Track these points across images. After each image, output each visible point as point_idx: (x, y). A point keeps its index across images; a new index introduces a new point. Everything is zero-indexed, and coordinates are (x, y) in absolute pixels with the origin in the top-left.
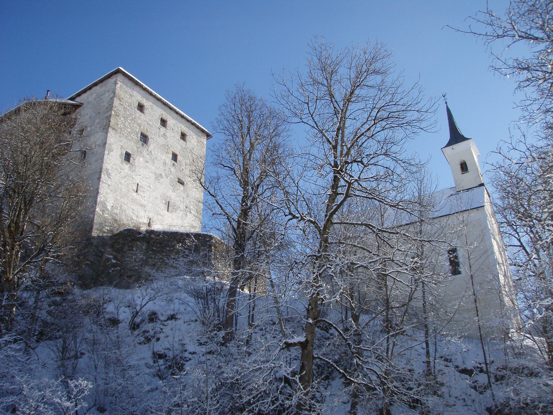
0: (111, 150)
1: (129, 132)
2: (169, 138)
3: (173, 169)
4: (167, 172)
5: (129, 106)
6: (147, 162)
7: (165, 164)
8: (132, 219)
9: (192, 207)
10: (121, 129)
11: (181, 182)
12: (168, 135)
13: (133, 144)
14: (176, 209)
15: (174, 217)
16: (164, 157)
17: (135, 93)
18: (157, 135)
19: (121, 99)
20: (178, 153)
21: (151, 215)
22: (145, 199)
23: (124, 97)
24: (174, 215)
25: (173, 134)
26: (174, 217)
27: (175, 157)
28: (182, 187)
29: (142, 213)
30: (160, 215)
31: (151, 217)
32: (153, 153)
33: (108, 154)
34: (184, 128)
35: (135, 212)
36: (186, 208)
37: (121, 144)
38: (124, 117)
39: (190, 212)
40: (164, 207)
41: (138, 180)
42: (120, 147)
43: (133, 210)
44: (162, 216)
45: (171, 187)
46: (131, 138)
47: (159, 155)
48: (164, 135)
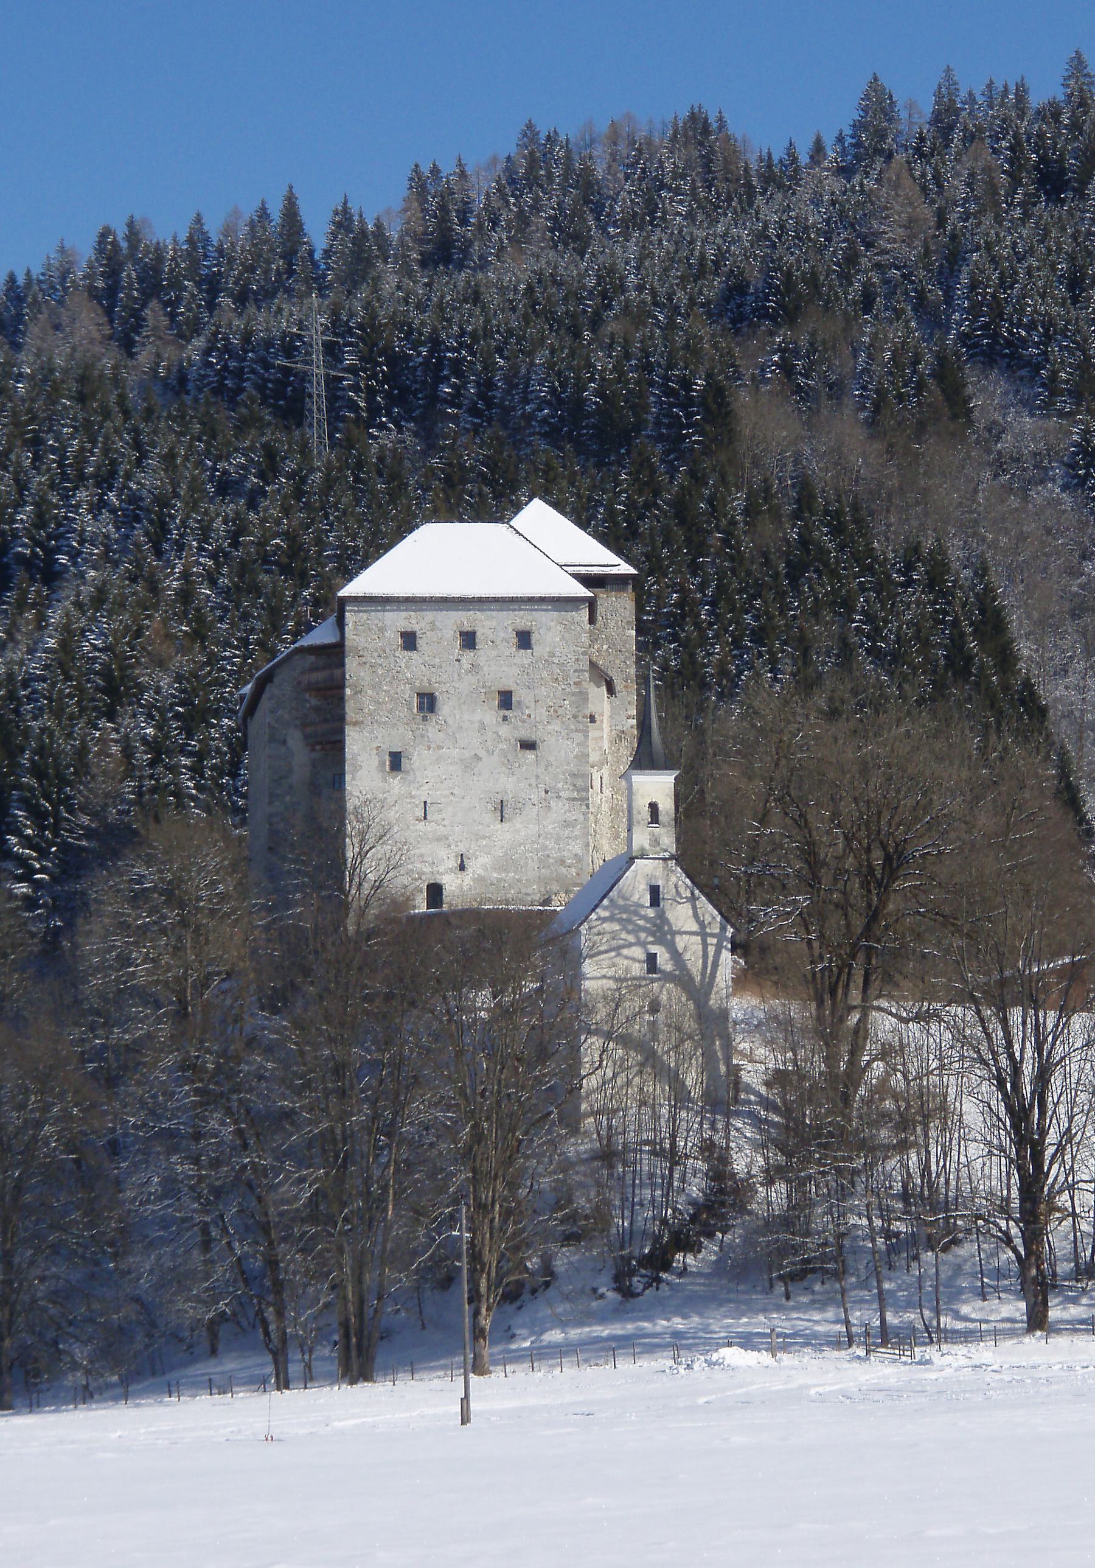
0: (357, 768)
1: (390, 711)
2: (485, 669)
3: (504, 730)
4: (489, 743)
5: (380, 656)
6: (440, 747)
7: (483, 726)
8: (423, 873)
9: (560, 785)
10: (370, 714)
11: (528, 745)
12: (482, 661)
13: (401, 730)
14: (519, 809)
15: (519, 826)
16: (478, 716)
17: (389, 616)
18: (456, 677)
19: (361, 653)
20: (512, 687)
21: (462, 848)
22: (446, 822)
23: (366, 645)
24: (518, 823)
25: (494, 653)
26: (519, 826)
27: (506, 700)
28: (530, 755)
29: (443, 853)
30: (484, 837)
31: (464, 851)
32: (450, 721)
33: (353, 779)
34: (522, 619)
35: (426, 859)
36: (547, 792)
37: (375, 745)
38: (374, 687)
39: (559, 797)
40: (489, 818)
41: (423, 795)
42: (375, 752)
43: (422, 855)
44: (489, 837)
45: (504, 769)
46: (394, 721)
47: (466, 717)
48: (475, 667)
